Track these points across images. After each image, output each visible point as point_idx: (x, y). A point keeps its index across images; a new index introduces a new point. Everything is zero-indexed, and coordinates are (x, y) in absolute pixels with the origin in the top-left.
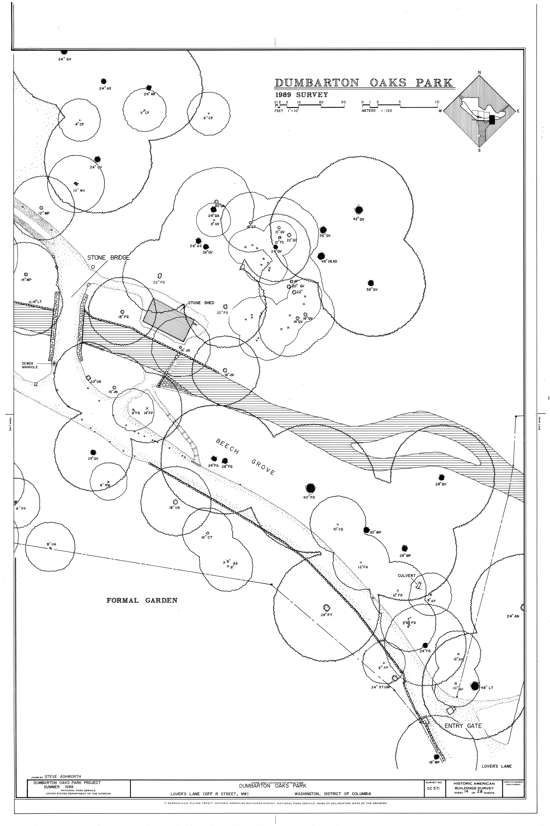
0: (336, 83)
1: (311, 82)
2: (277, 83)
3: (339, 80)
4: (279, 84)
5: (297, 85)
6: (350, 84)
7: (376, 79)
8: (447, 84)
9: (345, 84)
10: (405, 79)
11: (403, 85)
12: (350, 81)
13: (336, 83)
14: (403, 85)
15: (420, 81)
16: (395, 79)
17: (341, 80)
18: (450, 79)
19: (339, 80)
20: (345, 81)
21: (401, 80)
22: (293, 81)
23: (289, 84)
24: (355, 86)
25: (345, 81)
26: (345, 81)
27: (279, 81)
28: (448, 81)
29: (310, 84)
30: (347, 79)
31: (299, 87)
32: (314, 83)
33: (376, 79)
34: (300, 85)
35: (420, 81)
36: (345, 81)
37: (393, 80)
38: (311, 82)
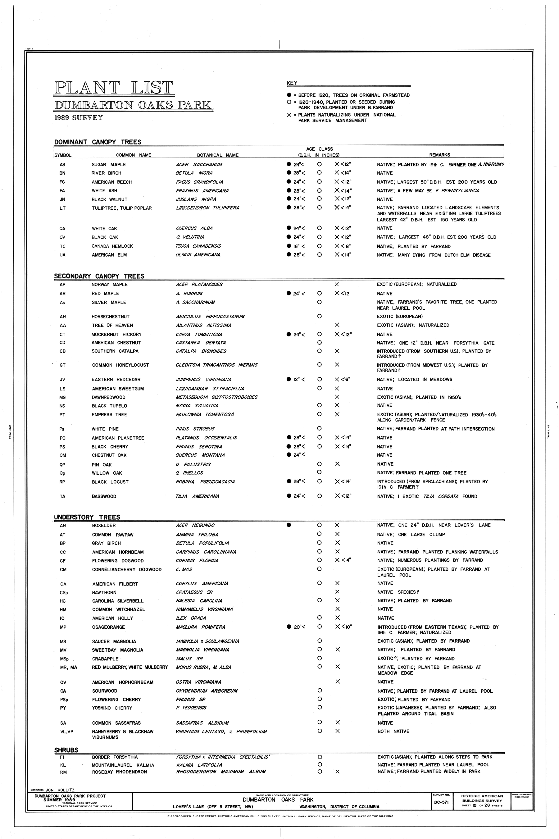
0: (111, 105)
1: (88, 105)
2: (57, 105)
3: (114, 102)
4: (59, 107)
5: (74, 107)
6: (124, 107)
7: (144, 102)
8: (206, 106)
9: (119, 107)
10: (172, 102)
11: (169, 107)
12: (124, 103)
13: (111, 105)
14: (169, 107)
15: (182, 103)
16: (162, 102)
17: (115, 103)
18: (209, 102)
19: (114, 102)
20: (119, 104)
21: (168, 102)
22: (71, 103)
23: (67, 107)
24: (129, 108)
25: (119, 104)
26: (119, 103)
27: (59, 103)
28: (206, 103)
29: (87, 107)
30: (121, 102)
31: (77, 109)
32: (91, 105)
33: (144, 102)
34: (78, 107)
35: (182, 103)
36: (119, 103)
37: (160, 103)
38: (88, 105)
